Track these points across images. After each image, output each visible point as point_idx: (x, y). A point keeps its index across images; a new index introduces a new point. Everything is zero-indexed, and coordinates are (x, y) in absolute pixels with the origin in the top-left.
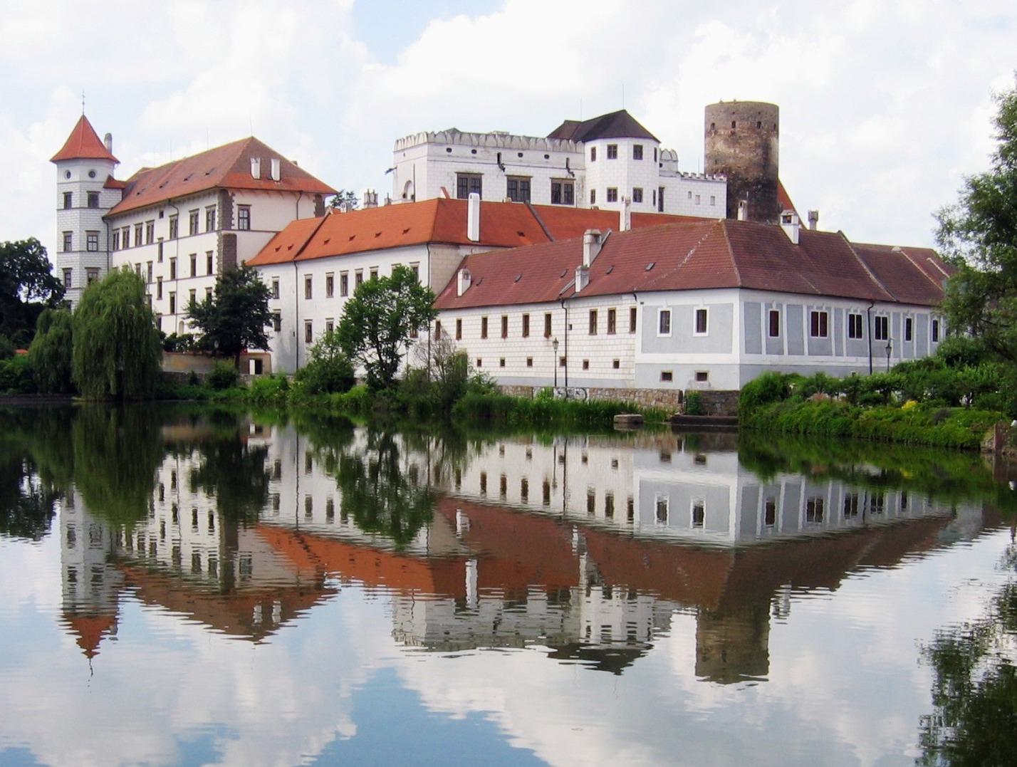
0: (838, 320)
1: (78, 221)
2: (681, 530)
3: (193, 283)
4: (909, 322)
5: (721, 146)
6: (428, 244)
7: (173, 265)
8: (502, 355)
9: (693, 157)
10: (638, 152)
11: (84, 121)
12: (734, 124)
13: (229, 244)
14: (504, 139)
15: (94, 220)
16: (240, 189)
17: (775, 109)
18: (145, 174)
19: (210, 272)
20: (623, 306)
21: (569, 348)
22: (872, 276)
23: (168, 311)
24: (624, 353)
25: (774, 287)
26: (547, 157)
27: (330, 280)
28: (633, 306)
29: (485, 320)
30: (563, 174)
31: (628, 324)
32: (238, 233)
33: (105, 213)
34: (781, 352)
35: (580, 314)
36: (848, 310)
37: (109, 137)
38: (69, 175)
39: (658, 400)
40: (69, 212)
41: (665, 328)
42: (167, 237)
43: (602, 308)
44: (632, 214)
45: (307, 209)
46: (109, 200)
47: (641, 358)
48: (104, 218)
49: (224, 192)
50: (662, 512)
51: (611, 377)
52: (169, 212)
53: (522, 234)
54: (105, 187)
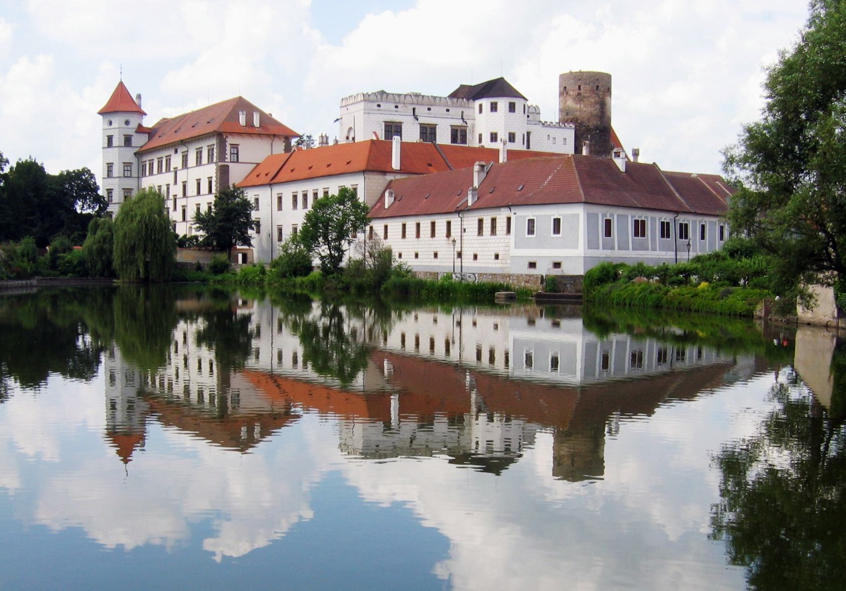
0: (653, 225)
1: (117, 156)
2: (542, 373)
3: (199, 200)
4: (703, 227)
5: (570, 103)
6: (364, 172)
7: (184, 187)
8: (416, 250)
9: (551, 111)
10: (512, 107)
11: (121, 84)
12: (580, 87)
13: (224, 172)
14: (418, 98)
15: (129, 155)
16: (231, 133)
17: (609, 77)
18: (165, 122)
19: (210, 191)
20: (501, 216)
21: (464, 245)
22: (677, 195)
23: (181, 219)
24: (502, 249)
25: (608, 202)
26: (448, 110)
27: (295, 197)
28: (509, 215)
29: (404, 226)
30: (459, 123)
31: (505, 228)
32: (230, 164)
33: (136, 150)
34: (613, 248)
35: (471, 222)
36: (660, 219)
37: (139, 97)
38: (111, 123)
39: (526, 282)
40: (110, 149)
41: (531, 231)
42: (180, 167)
43: (487, 217)
44: (508, 151)
45: (279, 147)
46: (139, 141)
47: (514, 252)
48: (135, 154)
49: (220, 135)
50: (529, 360)
51: (493, 266)
52: (181, 150)
53: (430, 165)
54: (136, 132)
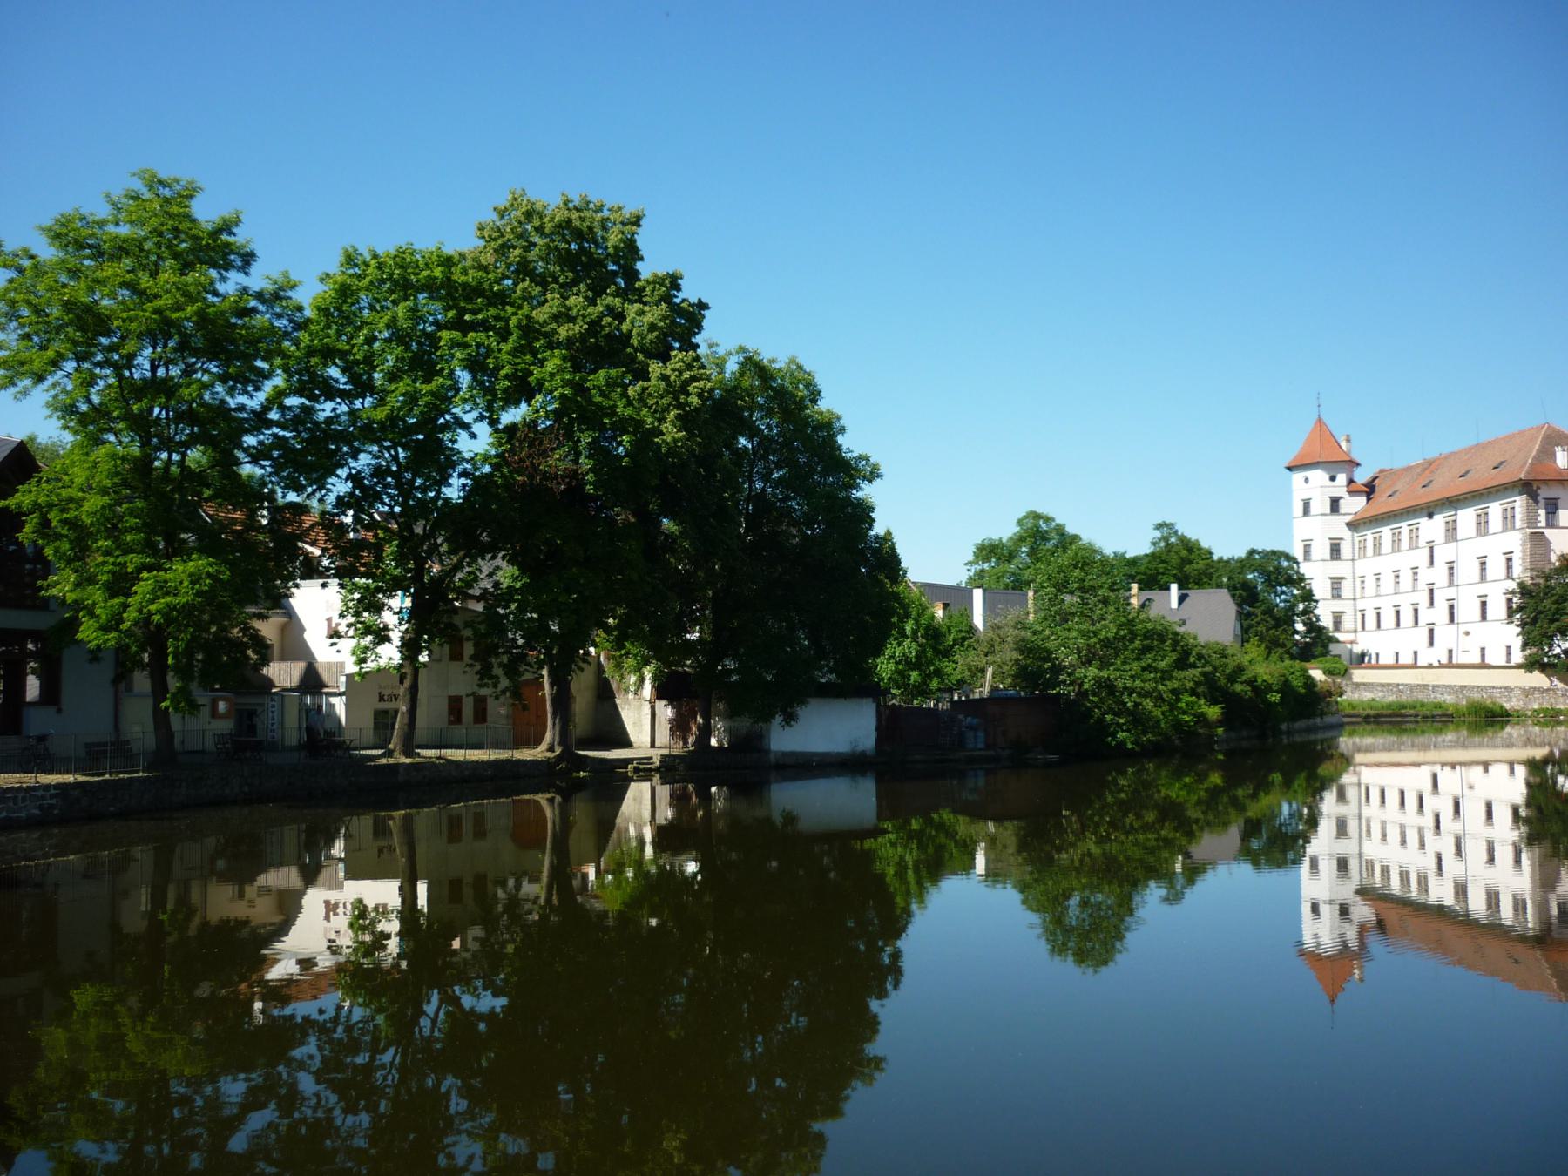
11: (1320, 421)
13: (1538, 542)
19: (1509, 576)
32: (1549, 533)
33: (1349, 518)
46: (1354, 505)
49: (1528, 487)
